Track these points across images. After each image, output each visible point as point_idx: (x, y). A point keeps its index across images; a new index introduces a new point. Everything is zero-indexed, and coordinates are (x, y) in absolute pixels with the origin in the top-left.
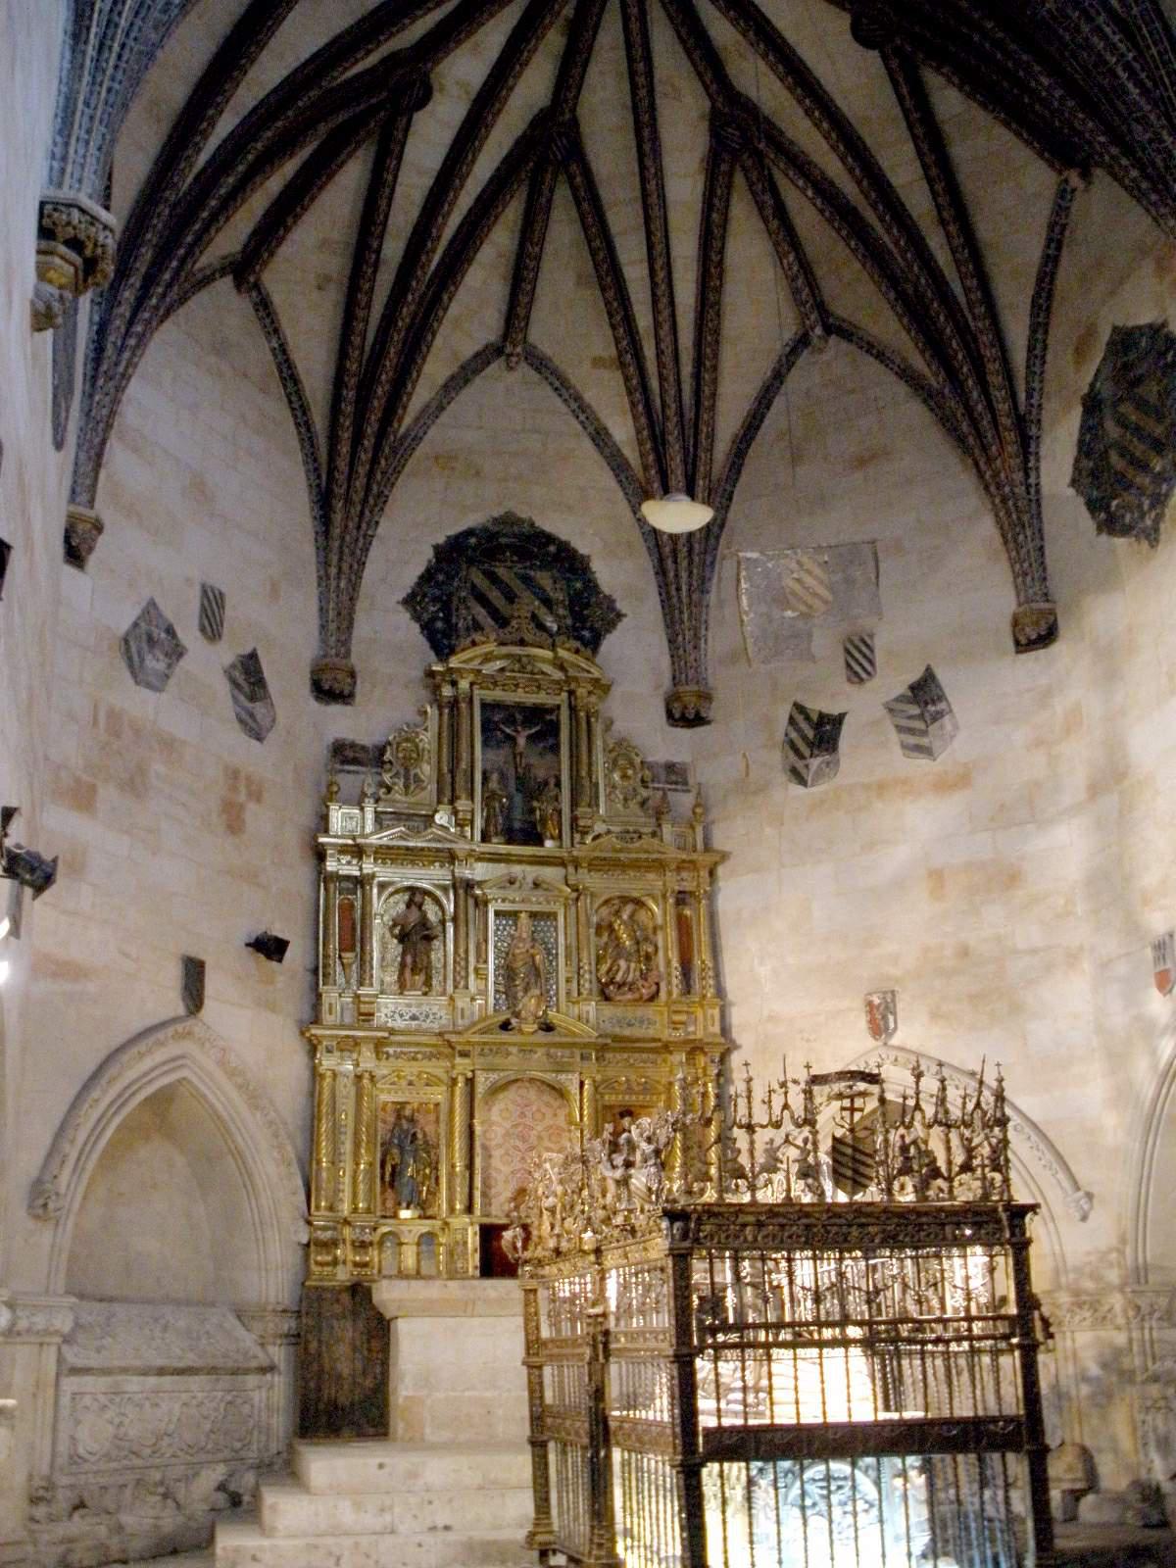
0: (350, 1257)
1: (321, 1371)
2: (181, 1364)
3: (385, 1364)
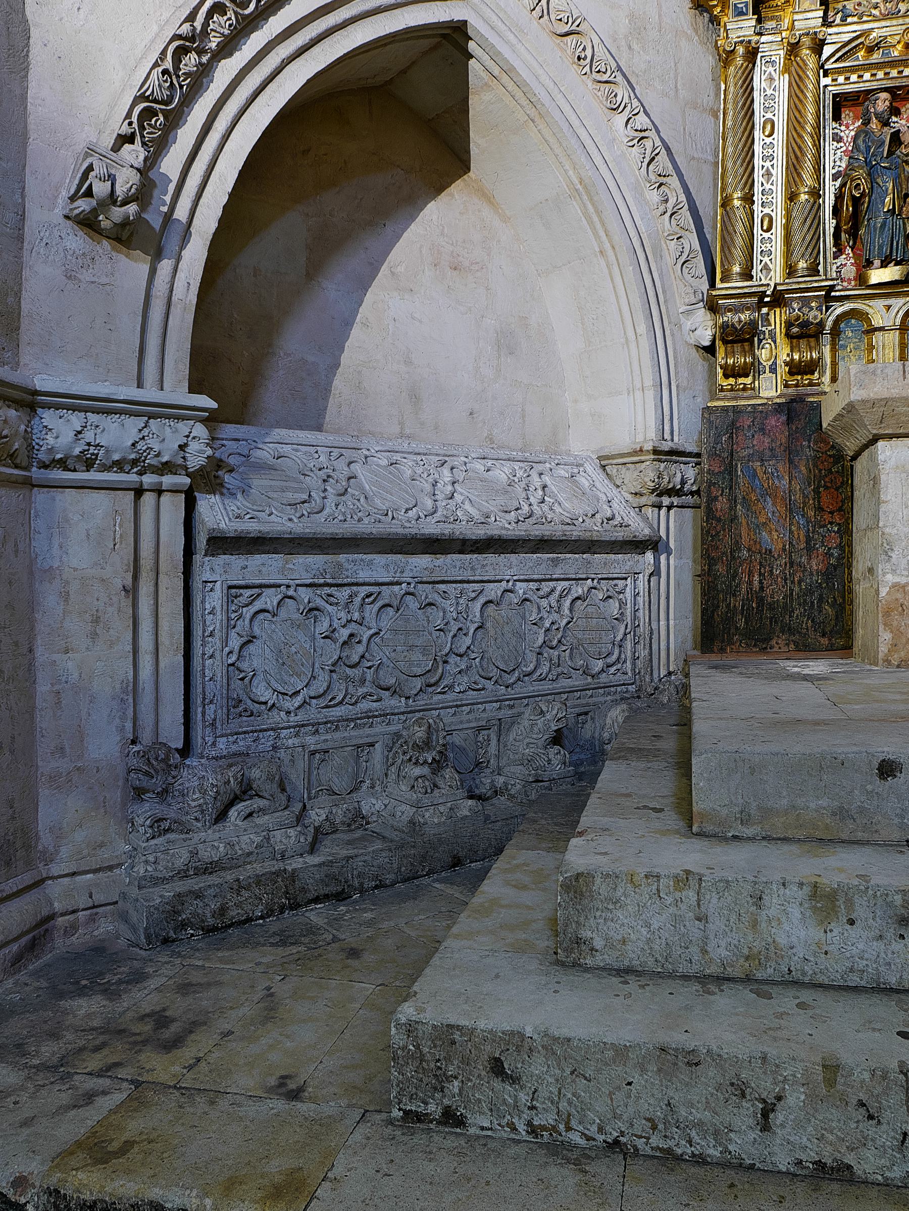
0: (784, 353)
1: (737, 546)
2: (480, 532)
3: (846, 531)
